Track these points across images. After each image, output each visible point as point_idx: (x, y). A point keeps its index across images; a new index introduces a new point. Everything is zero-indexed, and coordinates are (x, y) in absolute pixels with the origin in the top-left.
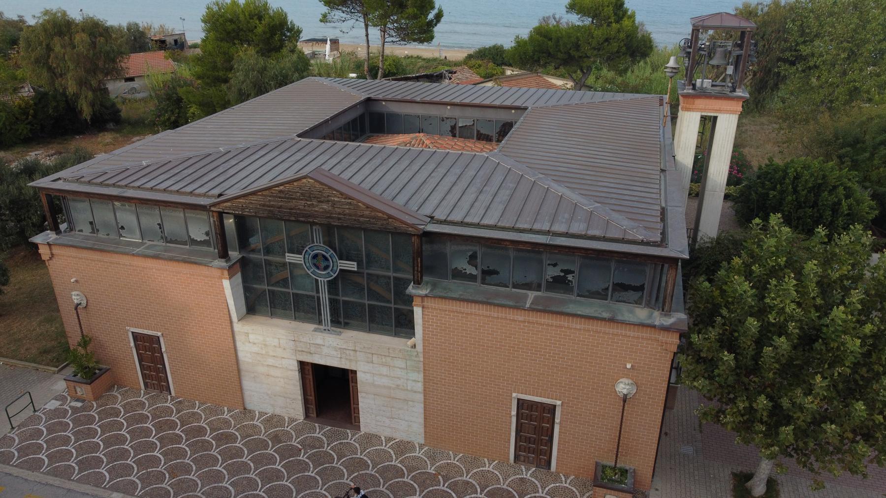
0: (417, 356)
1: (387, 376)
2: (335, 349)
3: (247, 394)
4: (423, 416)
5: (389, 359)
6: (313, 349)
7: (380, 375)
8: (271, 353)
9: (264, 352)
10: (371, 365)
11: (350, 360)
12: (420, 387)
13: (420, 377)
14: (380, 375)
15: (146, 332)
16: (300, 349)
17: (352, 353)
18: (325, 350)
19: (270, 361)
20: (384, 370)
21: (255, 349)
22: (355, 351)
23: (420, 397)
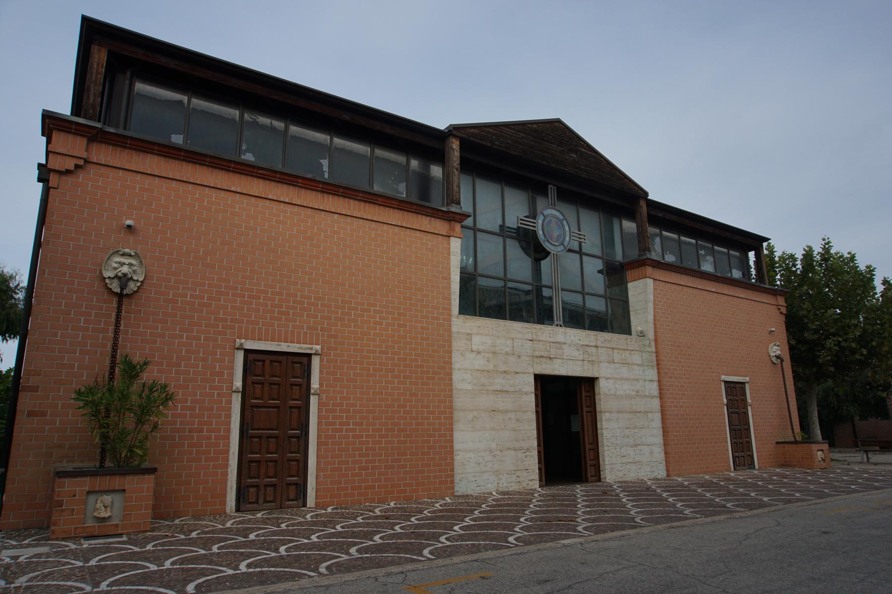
0: (650, 346)
1: (627, 379)
2: (579, 347)
3: (458, 458)
4: (661, 432)
5: (627, 353)
6: (553, 352)
7: (622, 379)
8: (502, 368)
9: (491, 367)
10: (612, 365)
11: (592, 362)
12: (654, 388)
13: (652, 374)
14: (622, 379)
15: (284, 347)
16: (537, 353)
17: (594, 350)
18: (568, 351)
19: (499, 382)
20: (624, 372)
21: (479, 363)
22: (596, 346)
23: (656, 403)
